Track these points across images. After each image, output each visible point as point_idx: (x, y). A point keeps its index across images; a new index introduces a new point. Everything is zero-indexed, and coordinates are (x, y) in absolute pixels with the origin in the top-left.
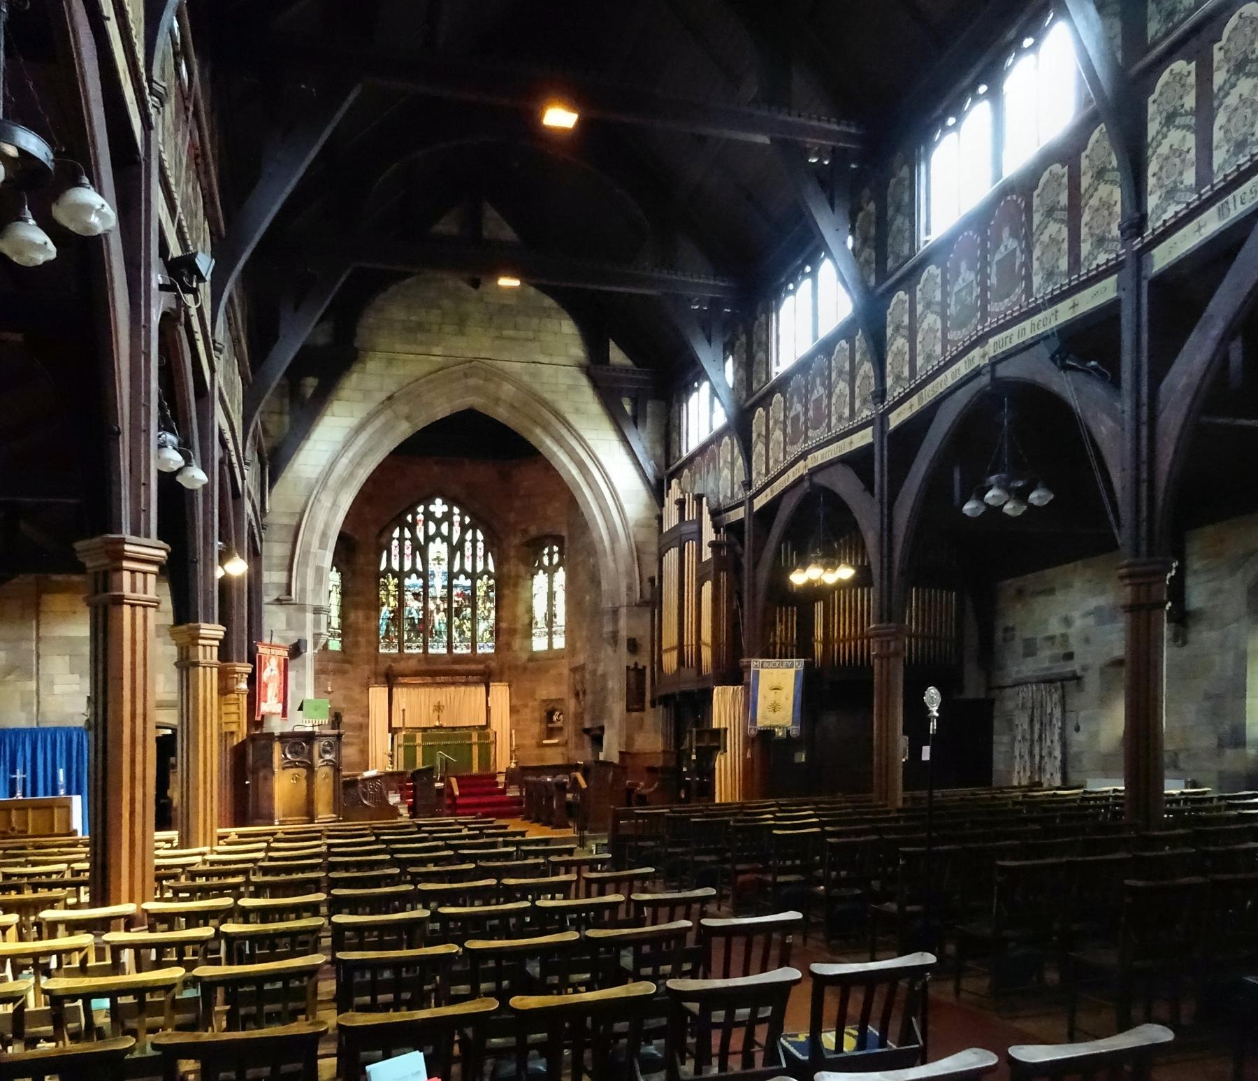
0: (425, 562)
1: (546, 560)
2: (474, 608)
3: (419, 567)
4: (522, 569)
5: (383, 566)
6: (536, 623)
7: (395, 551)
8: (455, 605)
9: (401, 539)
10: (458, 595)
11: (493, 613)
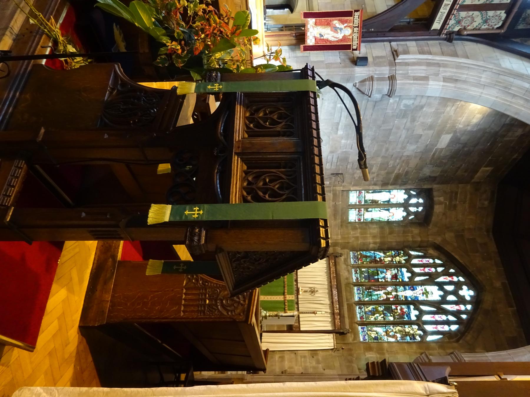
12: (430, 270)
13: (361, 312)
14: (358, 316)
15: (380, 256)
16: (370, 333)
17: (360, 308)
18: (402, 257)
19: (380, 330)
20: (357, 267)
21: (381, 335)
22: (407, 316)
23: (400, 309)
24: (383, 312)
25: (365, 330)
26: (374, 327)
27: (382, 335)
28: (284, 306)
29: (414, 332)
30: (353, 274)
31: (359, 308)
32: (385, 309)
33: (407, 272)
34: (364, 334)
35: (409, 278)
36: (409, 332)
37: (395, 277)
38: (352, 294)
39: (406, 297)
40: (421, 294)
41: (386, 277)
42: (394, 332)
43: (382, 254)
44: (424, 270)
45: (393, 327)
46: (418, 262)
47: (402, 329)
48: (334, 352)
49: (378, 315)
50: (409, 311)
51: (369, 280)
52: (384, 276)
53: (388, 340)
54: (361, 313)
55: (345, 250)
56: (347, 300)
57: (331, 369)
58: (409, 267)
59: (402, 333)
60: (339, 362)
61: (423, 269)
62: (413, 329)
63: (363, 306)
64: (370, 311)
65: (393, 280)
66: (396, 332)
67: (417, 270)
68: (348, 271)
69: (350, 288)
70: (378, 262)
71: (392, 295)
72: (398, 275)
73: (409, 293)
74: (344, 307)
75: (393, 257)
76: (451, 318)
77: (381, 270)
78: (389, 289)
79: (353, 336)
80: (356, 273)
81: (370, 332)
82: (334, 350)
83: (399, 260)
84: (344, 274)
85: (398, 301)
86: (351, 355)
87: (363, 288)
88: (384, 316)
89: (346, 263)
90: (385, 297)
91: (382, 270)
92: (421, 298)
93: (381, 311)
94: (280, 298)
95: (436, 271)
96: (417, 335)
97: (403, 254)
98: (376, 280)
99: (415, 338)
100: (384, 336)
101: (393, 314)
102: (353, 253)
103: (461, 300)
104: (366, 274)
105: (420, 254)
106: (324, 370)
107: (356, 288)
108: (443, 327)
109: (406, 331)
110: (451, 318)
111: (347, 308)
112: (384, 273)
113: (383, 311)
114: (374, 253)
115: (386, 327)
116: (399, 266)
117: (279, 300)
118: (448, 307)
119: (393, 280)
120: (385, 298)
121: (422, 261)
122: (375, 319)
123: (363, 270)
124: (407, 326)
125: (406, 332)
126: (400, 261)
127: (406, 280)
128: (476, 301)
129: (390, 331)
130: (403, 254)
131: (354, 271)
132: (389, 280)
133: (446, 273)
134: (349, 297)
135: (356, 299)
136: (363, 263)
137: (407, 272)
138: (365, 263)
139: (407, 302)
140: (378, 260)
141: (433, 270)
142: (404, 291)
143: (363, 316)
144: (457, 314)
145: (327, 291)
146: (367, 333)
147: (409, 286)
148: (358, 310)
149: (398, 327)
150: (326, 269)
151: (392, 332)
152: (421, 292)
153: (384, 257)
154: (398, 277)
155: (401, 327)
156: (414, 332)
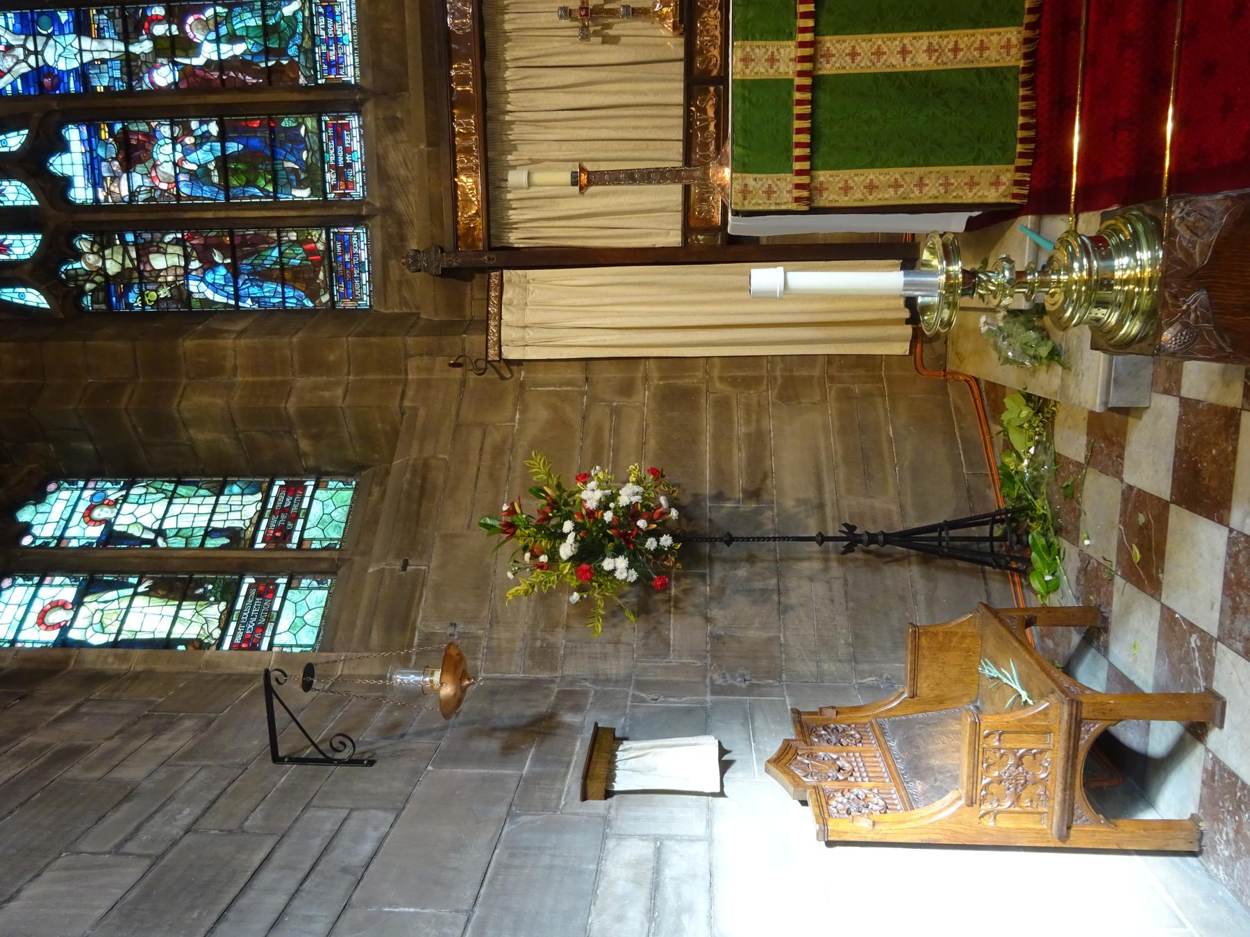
18: (88, 273)
52: (193, 157)
77: (207, 192)
80: (342, 172)
83: (108, 252)
89: (393, 230)
97: (84, 293)
98: (235, 130)
123: (303, 194)
126: (103, 248)
130: (84, 293)
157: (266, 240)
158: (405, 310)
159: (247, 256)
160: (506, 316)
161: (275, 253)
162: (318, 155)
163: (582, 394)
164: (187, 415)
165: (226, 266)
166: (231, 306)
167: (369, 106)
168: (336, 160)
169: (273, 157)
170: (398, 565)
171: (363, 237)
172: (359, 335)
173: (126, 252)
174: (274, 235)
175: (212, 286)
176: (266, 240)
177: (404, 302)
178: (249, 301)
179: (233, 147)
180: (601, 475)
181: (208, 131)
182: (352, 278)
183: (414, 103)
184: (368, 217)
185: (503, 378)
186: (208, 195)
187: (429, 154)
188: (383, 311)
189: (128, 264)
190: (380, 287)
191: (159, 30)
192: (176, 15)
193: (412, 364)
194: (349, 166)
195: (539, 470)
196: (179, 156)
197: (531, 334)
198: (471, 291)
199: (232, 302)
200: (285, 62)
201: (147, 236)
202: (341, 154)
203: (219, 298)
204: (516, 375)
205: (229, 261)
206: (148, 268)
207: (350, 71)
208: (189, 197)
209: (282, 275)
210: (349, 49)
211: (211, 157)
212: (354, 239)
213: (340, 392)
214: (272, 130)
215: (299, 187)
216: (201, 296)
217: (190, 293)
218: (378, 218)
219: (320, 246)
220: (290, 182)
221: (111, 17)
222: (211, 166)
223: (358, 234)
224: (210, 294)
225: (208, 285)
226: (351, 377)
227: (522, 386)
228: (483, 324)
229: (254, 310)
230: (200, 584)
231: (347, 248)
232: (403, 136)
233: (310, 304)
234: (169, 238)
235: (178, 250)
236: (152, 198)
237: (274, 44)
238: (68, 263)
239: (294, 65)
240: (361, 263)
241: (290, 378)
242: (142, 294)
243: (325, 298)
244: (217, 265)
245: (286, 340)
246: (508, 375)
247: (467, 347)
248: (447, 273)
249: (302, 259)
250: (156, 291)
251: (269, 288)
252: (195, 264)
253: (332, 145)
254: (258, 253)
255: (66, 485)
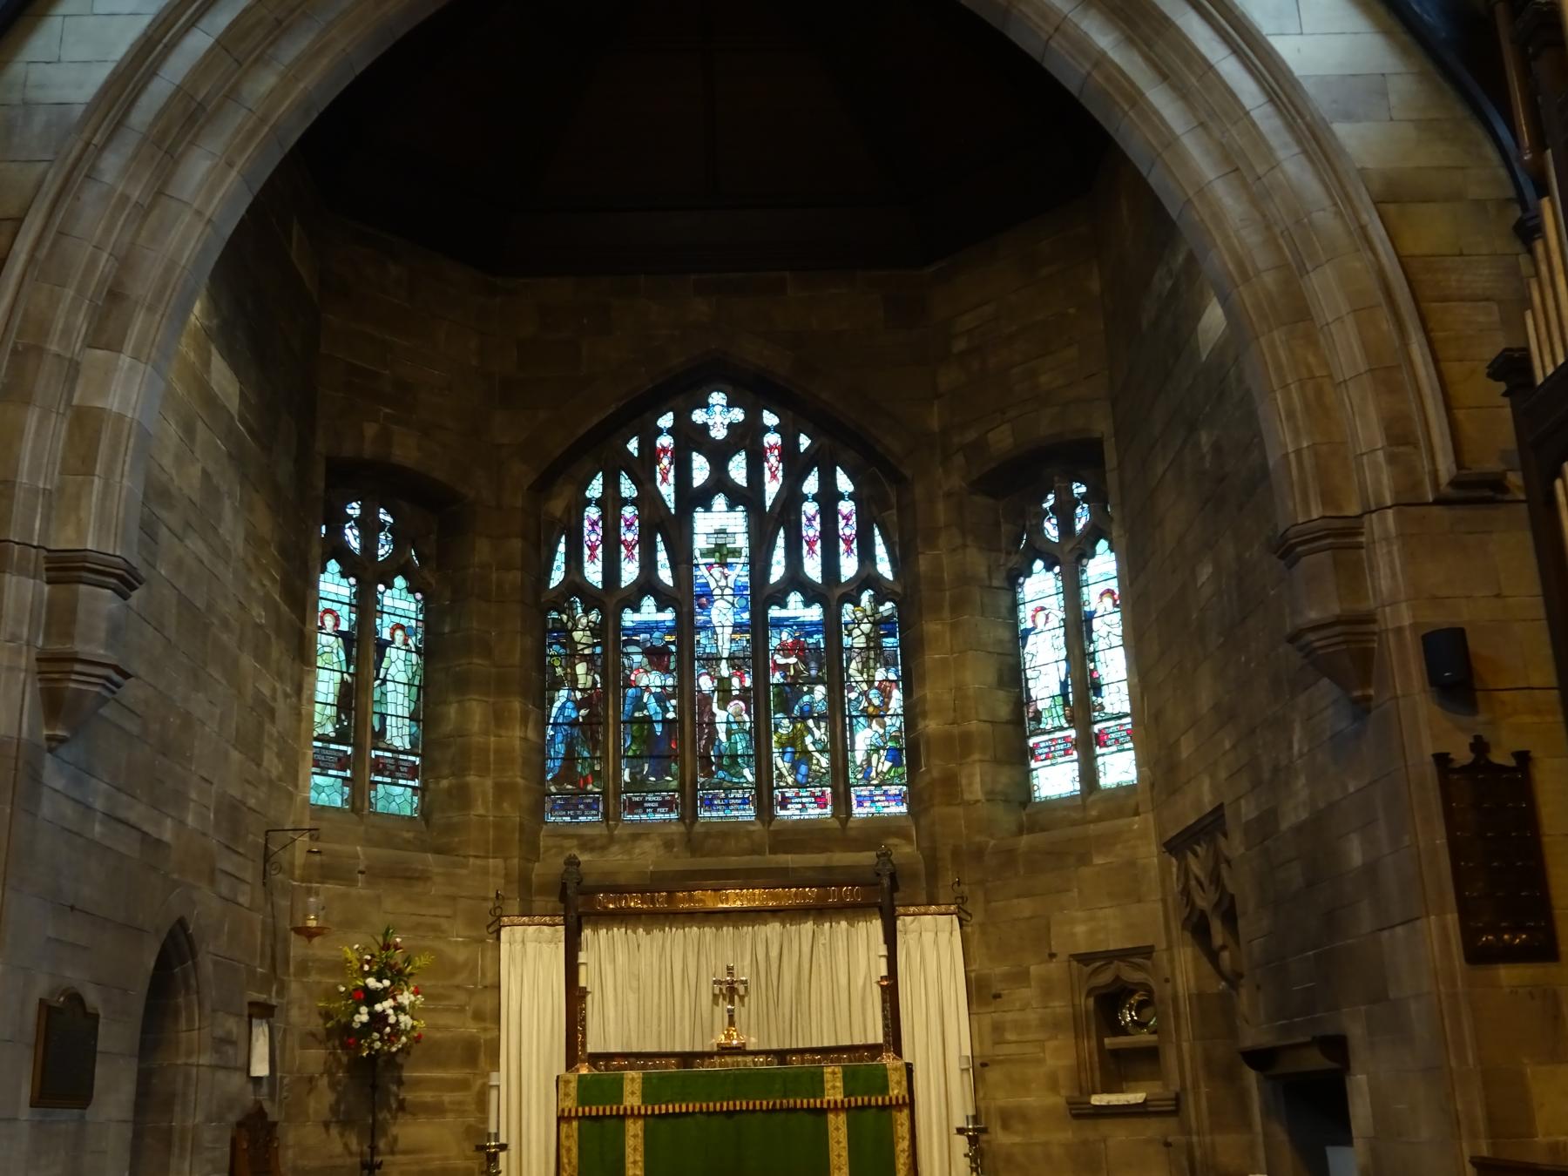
0: (682, 559)
1: (1051, 530)
2: (837, 684)
3: (665, 575)
4: (976, 560)
5: (557, 576)
6: (1038, 716)
7: (592, 536)
8: (777, 678)
9: (611, 503)
10: (785, 650)
11: (897, 695)
12: (632, 524)
13: (797, 800)
14: (813, 812)
15: (569, 704)
16: (877, 774)
17: (784, 803)
19: (864, 737)
20: (613, 802)
21: (881, 736)
22: (810, 635)
23: (785, 656)
24: (795, 718)
25: (866, 793)
26: (854, 757)
27: (881, 731)
28: (870, 1114)
29: (865, 620)
30: (644, 817)
31: (784, 807)
32: (787, 711)
33: (636, 609)
34: (883, 798)
35: (660, 608)
36: (867, 636)
37: (656, 657)
38: (730, 831)
39: (738, 627)
40: (726, 571)
41: (659, 690)
42: (870, 688)
43: (563, 693)
44: (630, 547)
45: (851, 689)
46: (599, 565)
47: (858, 659)
48: (970, 915)
49: (808, 740)
50: (791, 626)
51: (670, 757)
53: (897, 715)
54: (804, 800)
55: (542, 843)
56: (755, 850)
57: (1049, 930)
58: (613, 598)
59: (871, 662)
60: (1015, 901)
61: (627, 547)
62: (857, 623)
63: (776, 792)
64: (794, 768)
65: (672, 666)
66: (870, 683)
67: (630, 572)
68: (635, 837)
69: (707, 835)
70: (598, 715)
71: (729, 679)
72: (649, 645)
73: (723, 615)
74: (790, 865)
75: (572, 655)
76: (811, 485)
78: (706, 683)
79: (893, 841)
81: (873, 774)
82: (963, 915)
84: (647, 857)
85: (756, 658)
86: (978, 854)
87: (703, 784)
88: (813, 718)
89: (598, 843)
90: (736, 706)
91: (628, 701)
92: (739, 573)
93: (794, 727)
94: (838, 1128)
95: (633, 502)
96: (875, 611)
99: (886, 621)
100: (884, 726)
101: (803, 684)
102: (552, 810)
103: (746, 437)
104: (646, 767)
105: (562, 548)
106: (1052, 956)
107: (704, 814)
108: (844, 518)
109: (864, 645)
110: (811, 485)
111: (786, 852)
112: (642, 697)
113: (793, 720)
114: (555, 724)
115: (854, 713)
116: (610, 635)
117: (844, 1129)
118: (772, 488)
119: (672, 666)
120: (742, 704)
121: (593, 548)
122: (821, 752)
123: (626, 776)
124: (847, 641)
125: (868, 648)
127: (668, 616)
128: (748, 393)
129: (864, 704)
131: (632, 813)
132: (670, 681)
133: (643, 472)
134: (745, 843)
135: (749, 813)
136: (597, 776)
137: (636, 609)
138: (597, 768)
139: (758, 627)
140: (583, 712)
141: (629, 512)
142: (715, 633)
143: (813, 795)
144: (795, 468)
145: (728, 931)
146: (876, 786)
147: (694, 609)
148: (791, 813)
149: (851, 671)
150: (635, 932)
151: (871, 696)
152: (716, 571)
153: (574, 688)
154: (659, 644)
155: (849, 660)
156: (865, 620)
157: (594, 749)
158: (542, 850)
159: (584, 733)
160: (531, 929)
161: (586, 754)
162: (654, 789)
163: (475, 984)
164: (467, 704)
165: (577, 718)
166: (549, 719)
167: (682, 828)
168: (648, 802)
169: (651, 757)
170: (361, 868)
171: (595, 819)
172: (521, 824)
173: (589, 646)
174: (598, 754)
175: (563, 707)
176: (594, 749)
177: (548, 849)
178: (552, 733)
179: (658, 728)
180: (418, 1002)
181: (669, 711)
182: (566, 810)
183: (683, 862)
184: (608, 825)
185: (488, 927)
186: (626, 708)
187: (646, 873)
188: (542, 833)
189: (580, 647)
190: (559, 833)
191: (735, 682)
192: (744, 694)
193: (499, 862)
194: (645, 812)
195: (421, 961)
196: (653, 690)
197: (518, 947)
198: (553, 902)
199: (551, 721)
200: (714, 768)
201: (599, 662)
202: (652, 805)
203: (554, 711)
204: (491, 936)
205: (581, 720)
206: (576, 661)
207: (707, 814)
208: (625, 696)
209: (570, 758)
210: (721, 814)
211: (652, 713)
212: (594, 812)
213: (481, 811)
214: (670, 757)
215: (631, 773)
216: (556, 698)
217: (558, 691)
218: (606, 832)
219: (590, 787)
220: (635, 767)
221: (744, 649)
222: (645, 712)
223: (597, 815)
224: (557, 704)
225: (564, 704)
226: (491, 818)
227: (482, 941)
228: (527, 911)
229: (545, 736)
230: (348, 717)
231: (589, 807)
232: (662, 852)
233: (549, 777)
234: (597, 677)
235: (589, 684)
236: (625, 668)
237: (725, 761)
238: (581, 603)
239: (711, 774)
240: (576, 817)
241: (492, 775)
242: (559, 655)
243: (553, 789)
244: (578, 711)
245: (519, 773)
246: (491, 930)
247: (511, 902)
248: (564, 887)
249: (581, 773)
250: (561, 666)
251: (561, 748)
252: (579, 695)
253: (659, 799)
254: (584, 743)
255: (420, 606)
